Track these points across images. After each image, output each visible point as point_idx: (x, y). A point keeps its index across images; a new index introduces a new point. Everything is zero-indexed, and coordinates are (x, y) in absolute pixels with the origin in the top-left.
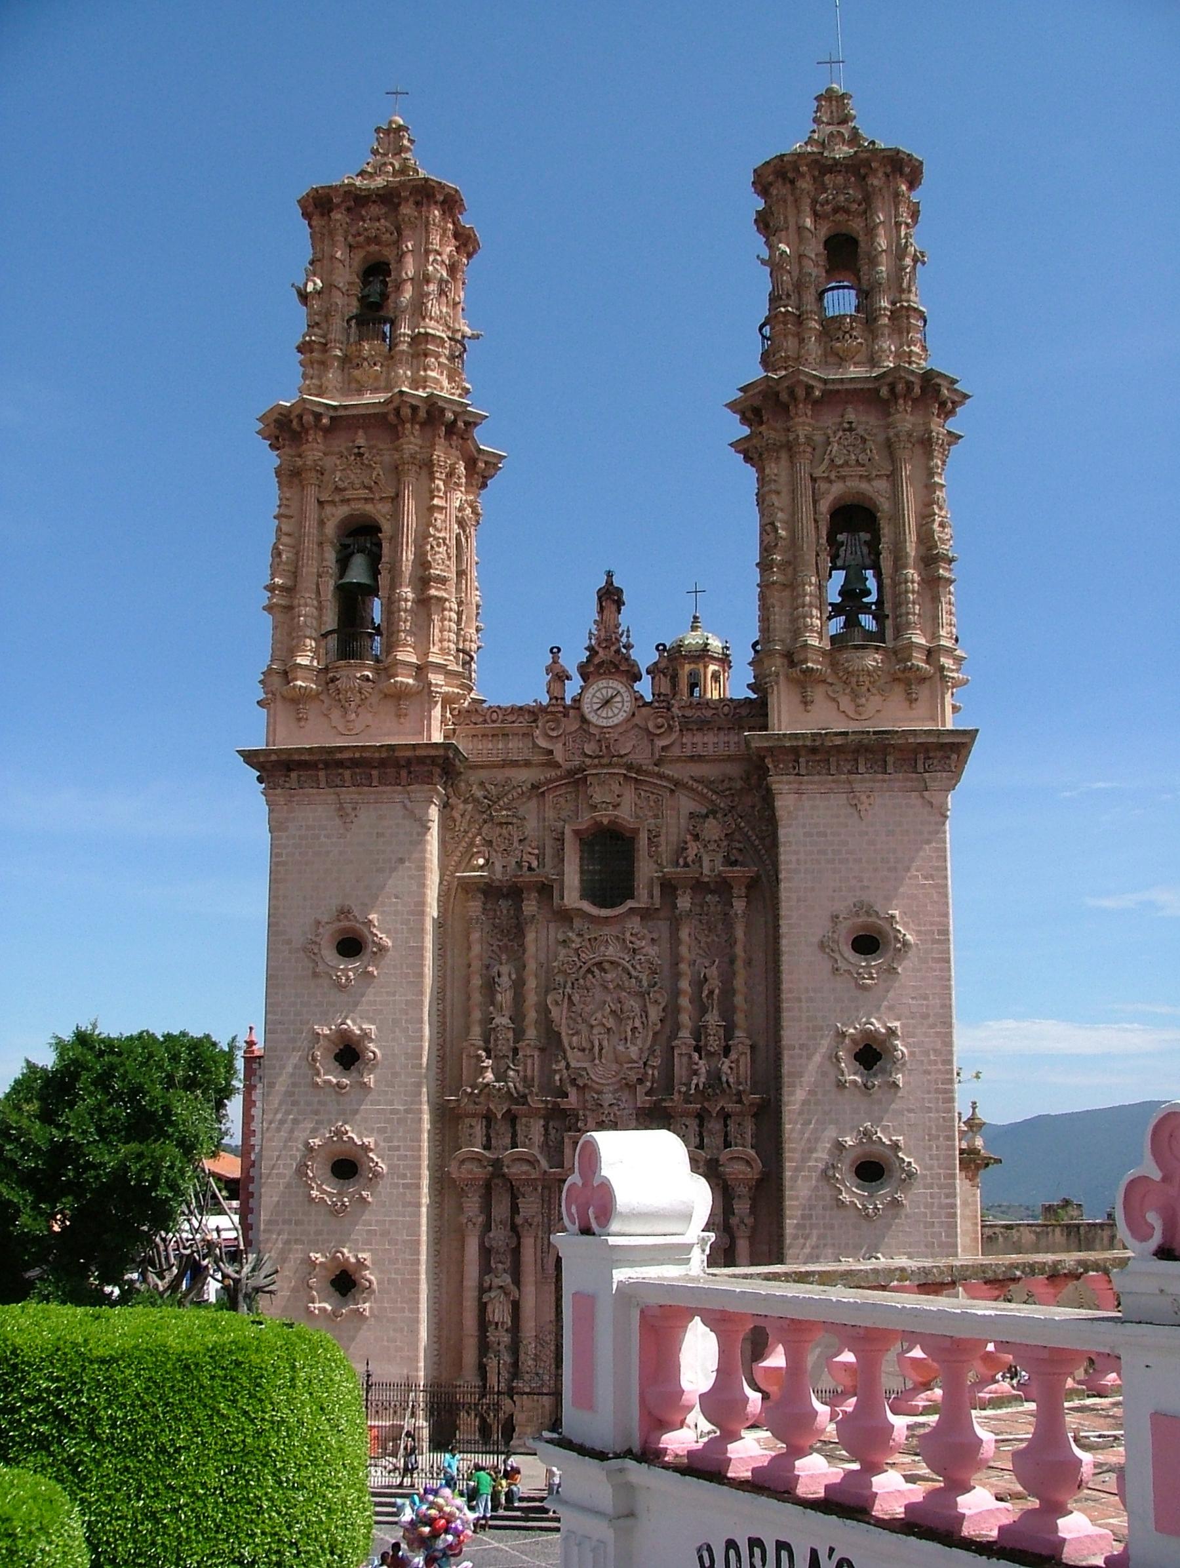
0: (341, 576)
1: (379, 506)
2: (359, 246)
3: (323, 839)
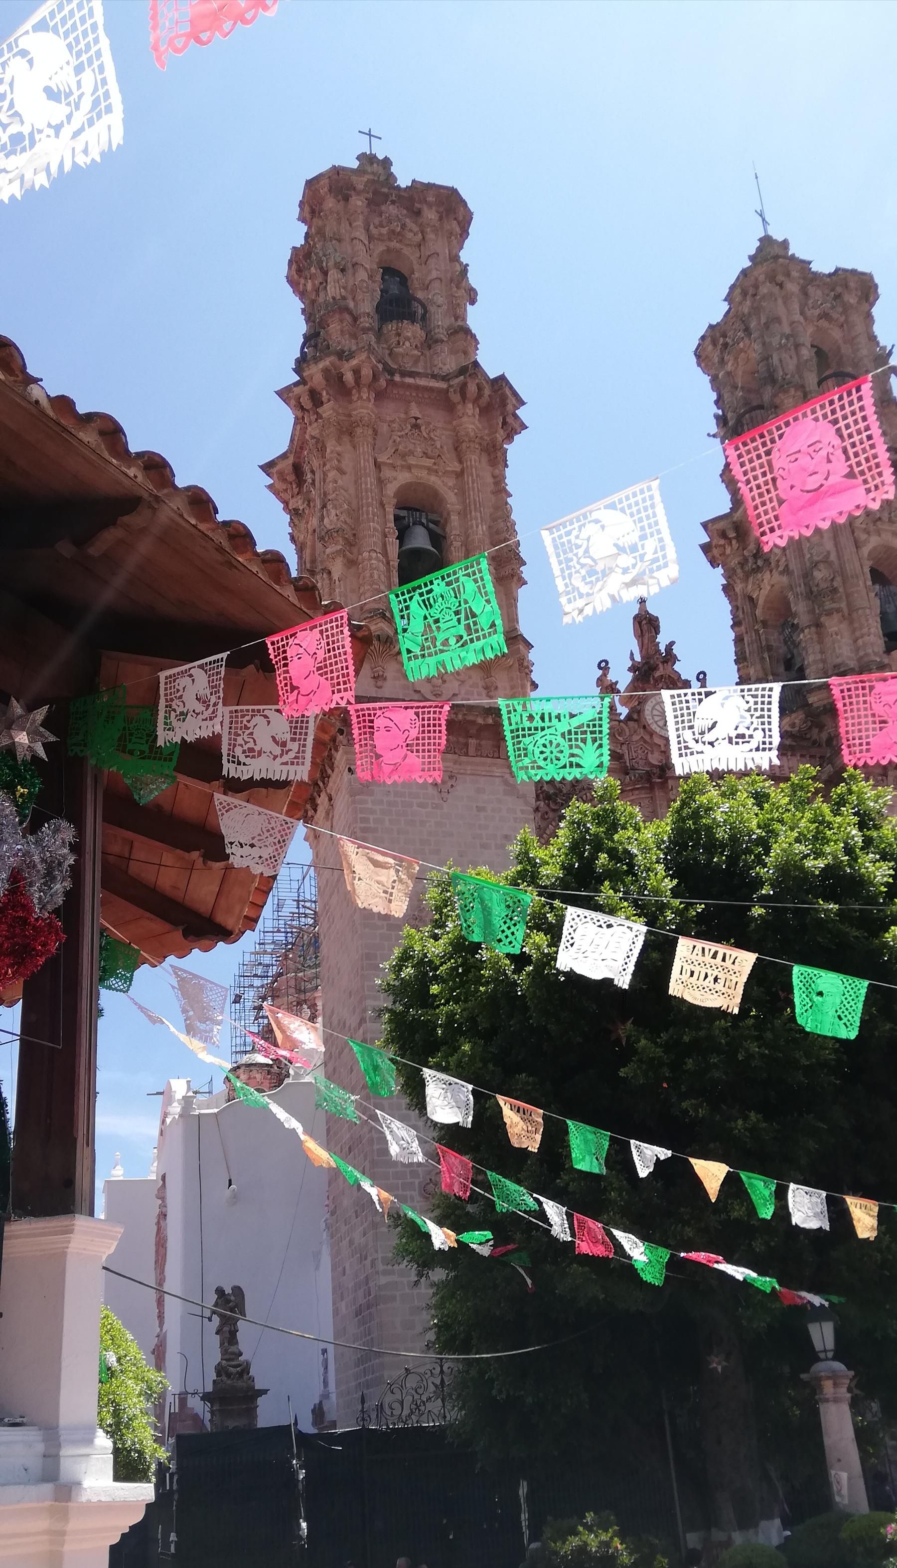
0: (400, 546)
1: (446, 480)
2: (380, 238)
3: (415, 808)
